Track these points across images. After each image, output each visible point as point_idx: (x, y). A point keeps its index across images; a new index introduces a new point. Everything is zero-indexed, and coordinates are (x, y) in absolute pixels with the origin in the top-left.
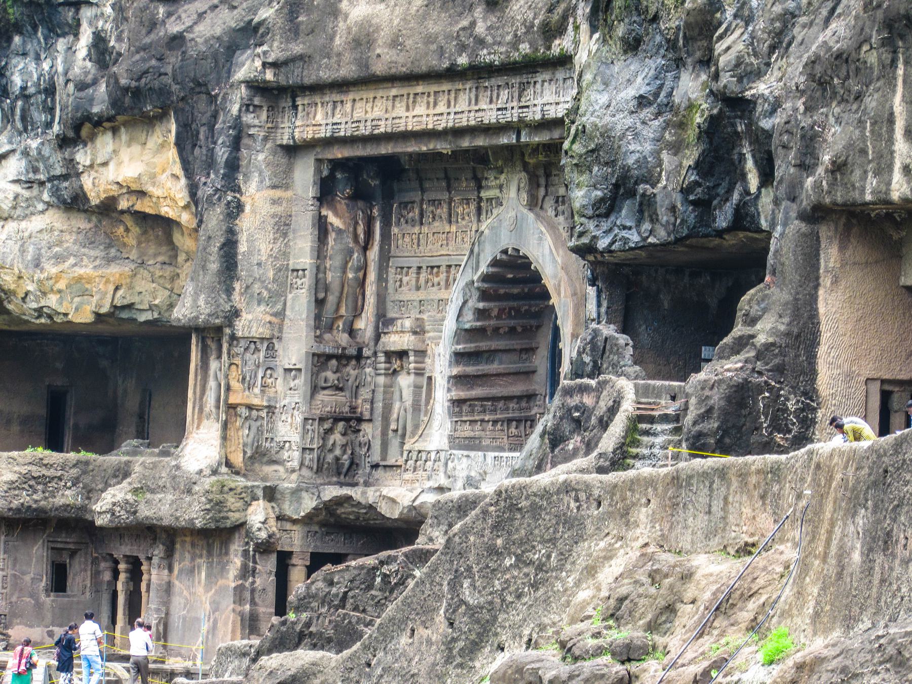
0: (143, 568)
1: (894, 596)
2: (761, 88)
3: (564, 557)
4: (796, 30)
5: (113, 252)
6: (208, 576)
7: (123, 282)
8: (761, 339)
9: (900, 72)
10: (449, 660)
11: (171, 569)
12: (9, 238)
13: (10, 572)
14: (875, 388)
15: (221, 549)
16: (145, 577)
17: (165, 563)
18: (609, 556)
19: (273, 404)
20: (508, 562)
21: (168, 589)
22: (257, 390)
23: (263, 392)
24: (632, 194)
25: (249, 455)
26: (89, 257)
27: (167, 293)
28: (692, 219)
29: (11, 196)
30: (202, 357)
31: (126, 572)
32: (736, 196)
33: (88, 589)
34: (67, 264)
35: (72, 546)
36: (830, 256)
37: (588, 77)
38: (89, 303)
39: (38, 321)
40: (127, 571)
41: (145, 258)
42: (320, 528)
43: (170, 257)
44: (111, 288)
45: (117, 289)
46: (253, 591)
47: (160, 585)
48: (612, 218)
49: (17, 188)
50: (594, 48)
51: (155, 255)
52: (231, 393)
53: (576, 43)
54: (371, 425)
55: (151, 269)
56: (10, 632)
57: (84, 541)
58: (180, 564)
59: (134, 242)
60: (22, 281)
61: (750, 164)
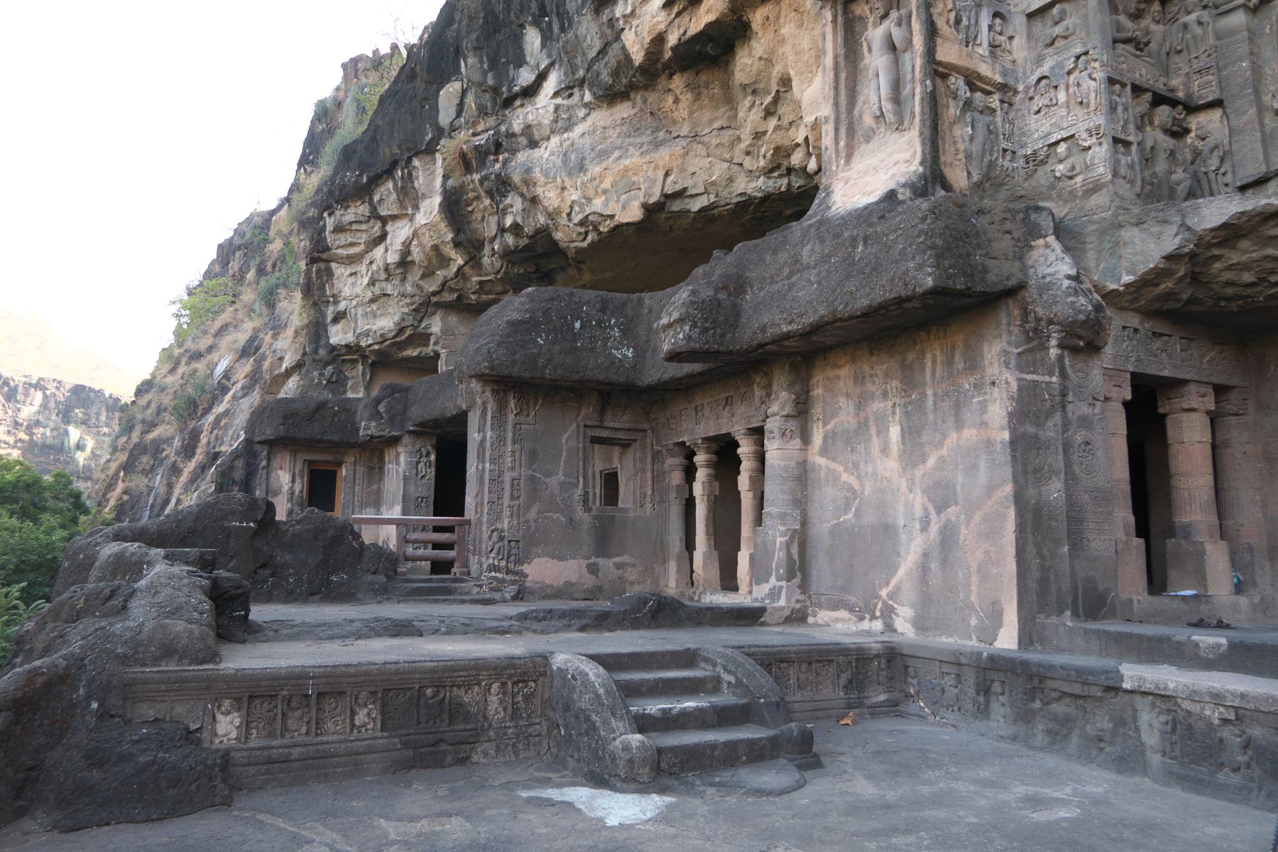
0: (739, 451)
5: (661, 134)
6: (910, 433)
7: (675, 165)
11: (806, 438)
12: (552, 153)
13: (525, 472)
15: (949, 363)
16: (746, 466)
17: (792, 425)
19: (1011, 82)
21: (803, 477)
22: (983, 50)
23: (993, 54)
25: (975, 178)
26: (634, 145)
27: (726, 165)
29: (552, 108)
30: (846, 39)
31: (707, 466)
33: (648, 499)
34: (611, 159)
35: (621, 435)
38: (636, 198)
39: (585, 244)
40: (709, 464)
41: (699, 129)
42: (1142, 323)
43: (729, 118)
44: (661, 173)
45: (667, 174)
46: (1067, 446)
47: (786, 468)
49: (559, 101)
51: (710, 122)
52: (939, 41)
54: (1216, 114)
55: (706, 139)
56: (526, 568)
57: (640, 426)
58: (825, 424)
59: (685, 114)
60: (566, 193)
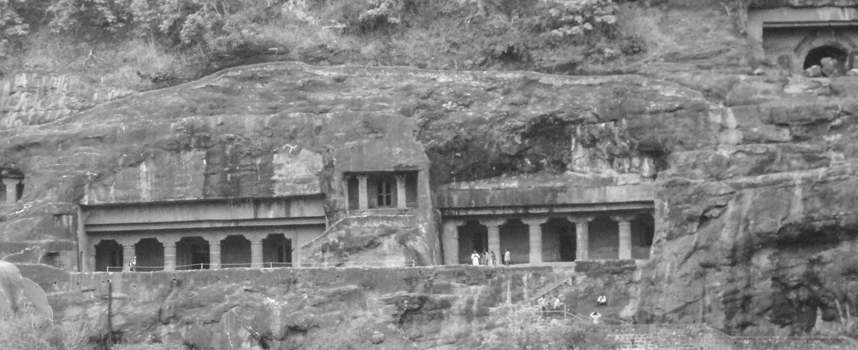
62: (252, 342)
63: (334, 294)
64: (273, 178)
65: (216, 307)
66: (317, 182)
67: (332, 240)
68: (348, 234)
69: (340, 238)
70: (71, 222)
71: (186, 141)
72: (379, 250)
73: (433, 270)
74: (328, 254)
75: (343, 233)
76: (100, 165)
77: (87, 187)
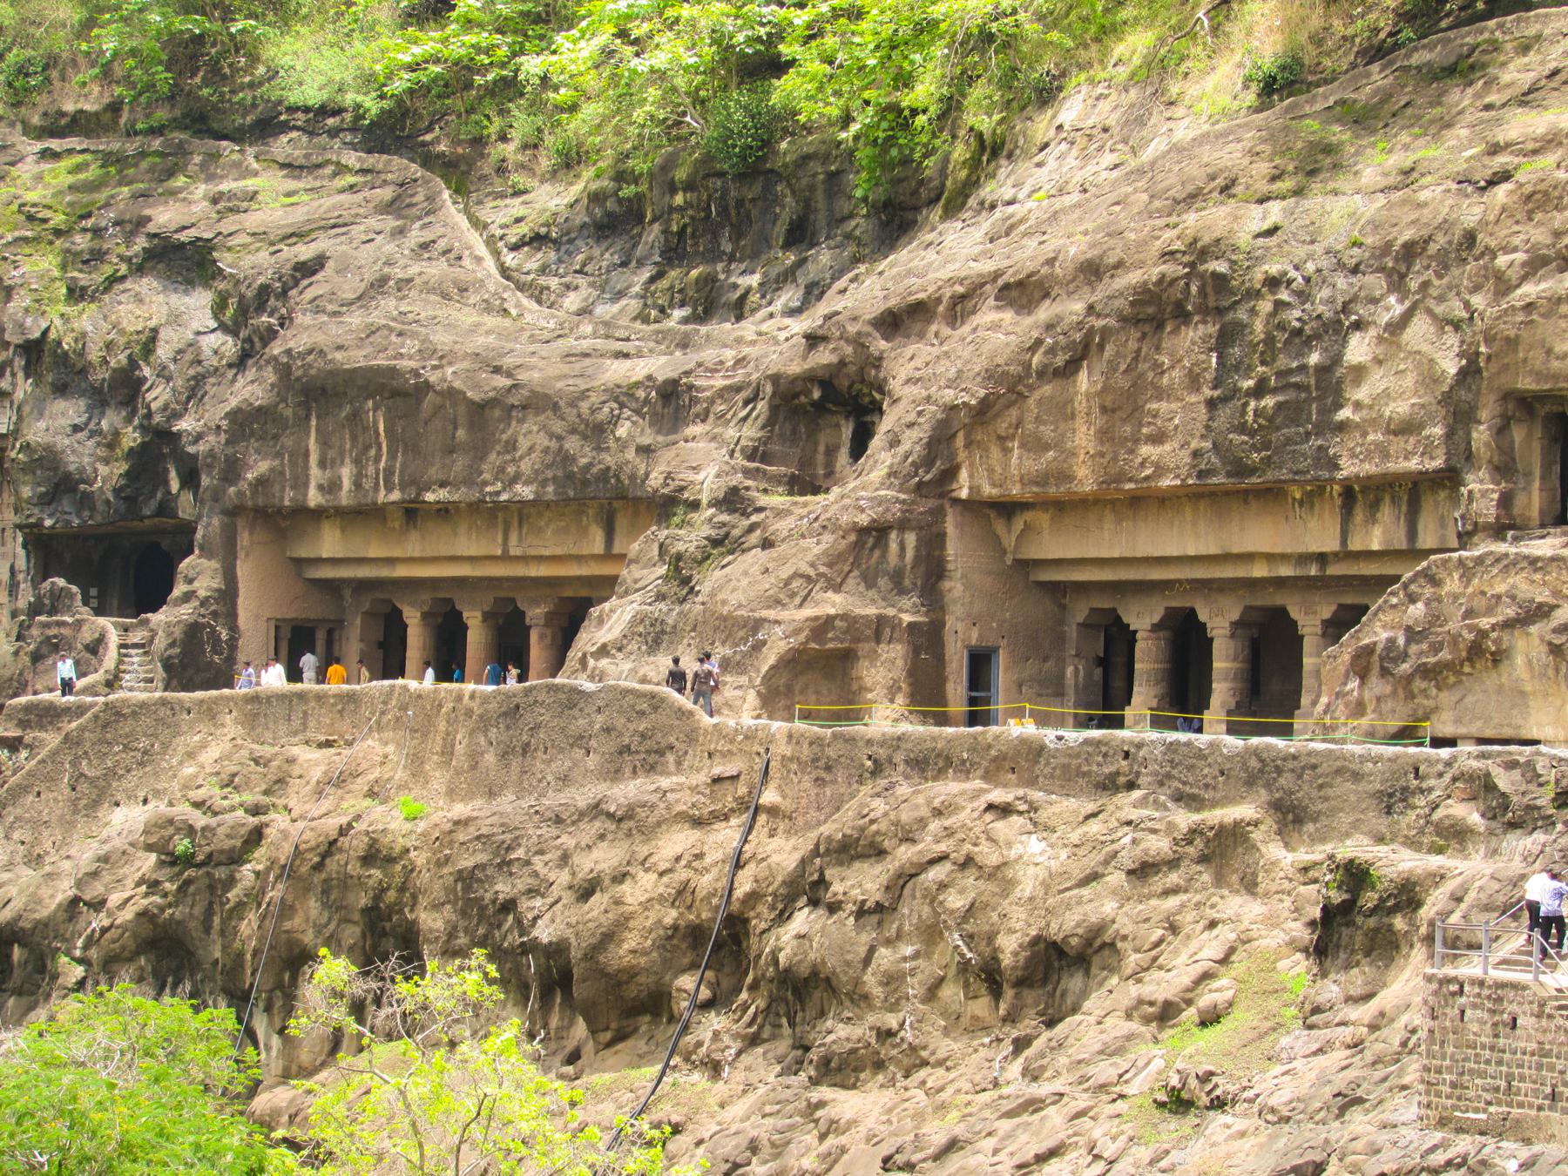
1: (540, 781)
2: (185, 425)
3: (165, 746)
4: (208, 387)
8: (202, 593)
9: (314, 422)
10: (76, 812)
14: (273, 624)
18: (204, 745)
20: (116, 749)
24: (74, 490)
28: (122, 507)
32: (159, 495)
36: (244, 539)
37: (27, 409)
48: (54, 505)
50: (29, 390)
53: (14, 385)
61: (173, 474)
62: (966, 985)
63: (1194, 832)
64: (1345, 413)
65: (904, 854)
66: (1438, 431)
67: (1384, 635)
68: (1435, 619)
69: (1412, 635)
70: (910, 554)
71: (1176, 293)
72: (1505, 675)
73: (1448, 764)
74: (1377, 686)
75: (1418, 610)
76: (990, 375)
77: (960, 441)
